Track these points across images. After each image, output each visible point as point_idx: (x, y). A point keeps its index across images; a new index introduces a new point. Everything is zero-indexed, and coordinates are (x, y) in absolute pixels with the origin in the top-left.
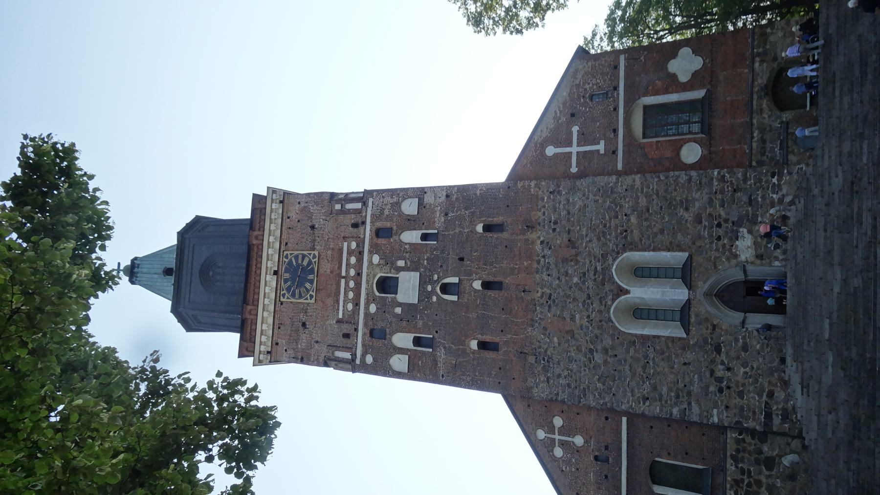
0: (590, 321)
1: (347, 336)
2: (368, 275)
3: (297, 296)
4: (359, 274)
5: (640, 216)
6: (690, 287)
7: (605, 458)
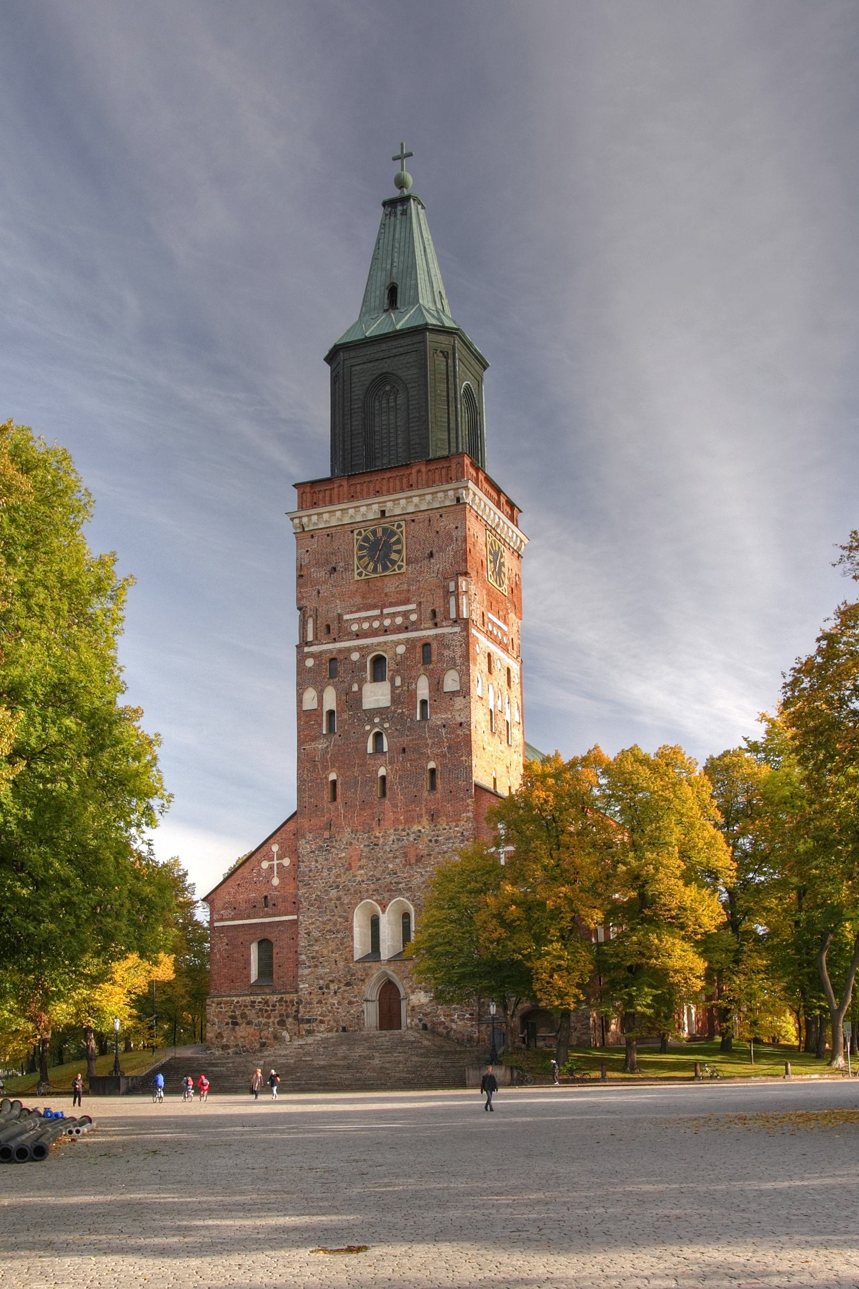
1: (328, 627)
2: (385, 643)
3: (361, 553)
4: (386, 631)
6: (389, 961)
7: (267, 904)
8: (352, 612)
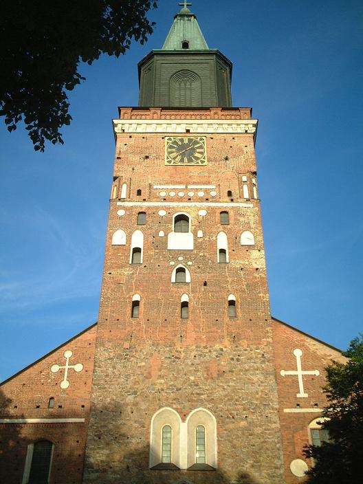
0: (159, 391)
1: (139, 193)
3: (169, 150)
5: (246, 428)
8: (160, 184)
